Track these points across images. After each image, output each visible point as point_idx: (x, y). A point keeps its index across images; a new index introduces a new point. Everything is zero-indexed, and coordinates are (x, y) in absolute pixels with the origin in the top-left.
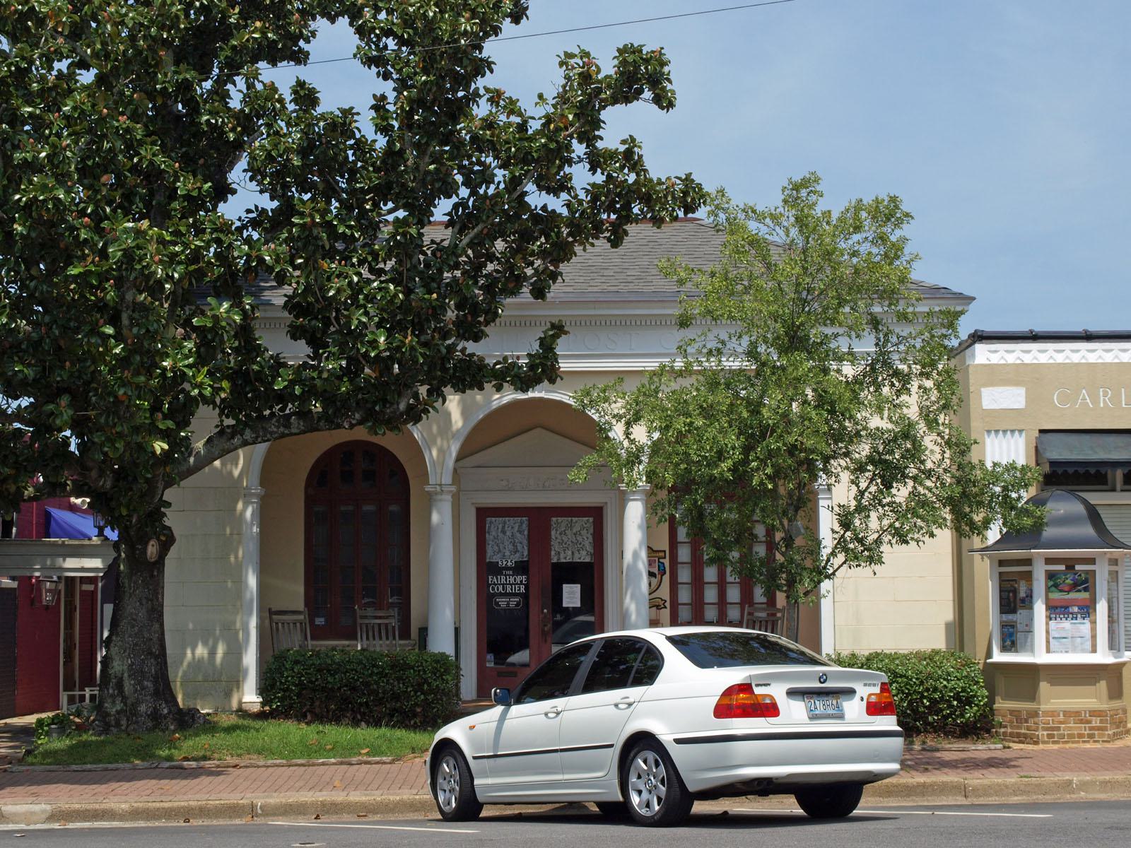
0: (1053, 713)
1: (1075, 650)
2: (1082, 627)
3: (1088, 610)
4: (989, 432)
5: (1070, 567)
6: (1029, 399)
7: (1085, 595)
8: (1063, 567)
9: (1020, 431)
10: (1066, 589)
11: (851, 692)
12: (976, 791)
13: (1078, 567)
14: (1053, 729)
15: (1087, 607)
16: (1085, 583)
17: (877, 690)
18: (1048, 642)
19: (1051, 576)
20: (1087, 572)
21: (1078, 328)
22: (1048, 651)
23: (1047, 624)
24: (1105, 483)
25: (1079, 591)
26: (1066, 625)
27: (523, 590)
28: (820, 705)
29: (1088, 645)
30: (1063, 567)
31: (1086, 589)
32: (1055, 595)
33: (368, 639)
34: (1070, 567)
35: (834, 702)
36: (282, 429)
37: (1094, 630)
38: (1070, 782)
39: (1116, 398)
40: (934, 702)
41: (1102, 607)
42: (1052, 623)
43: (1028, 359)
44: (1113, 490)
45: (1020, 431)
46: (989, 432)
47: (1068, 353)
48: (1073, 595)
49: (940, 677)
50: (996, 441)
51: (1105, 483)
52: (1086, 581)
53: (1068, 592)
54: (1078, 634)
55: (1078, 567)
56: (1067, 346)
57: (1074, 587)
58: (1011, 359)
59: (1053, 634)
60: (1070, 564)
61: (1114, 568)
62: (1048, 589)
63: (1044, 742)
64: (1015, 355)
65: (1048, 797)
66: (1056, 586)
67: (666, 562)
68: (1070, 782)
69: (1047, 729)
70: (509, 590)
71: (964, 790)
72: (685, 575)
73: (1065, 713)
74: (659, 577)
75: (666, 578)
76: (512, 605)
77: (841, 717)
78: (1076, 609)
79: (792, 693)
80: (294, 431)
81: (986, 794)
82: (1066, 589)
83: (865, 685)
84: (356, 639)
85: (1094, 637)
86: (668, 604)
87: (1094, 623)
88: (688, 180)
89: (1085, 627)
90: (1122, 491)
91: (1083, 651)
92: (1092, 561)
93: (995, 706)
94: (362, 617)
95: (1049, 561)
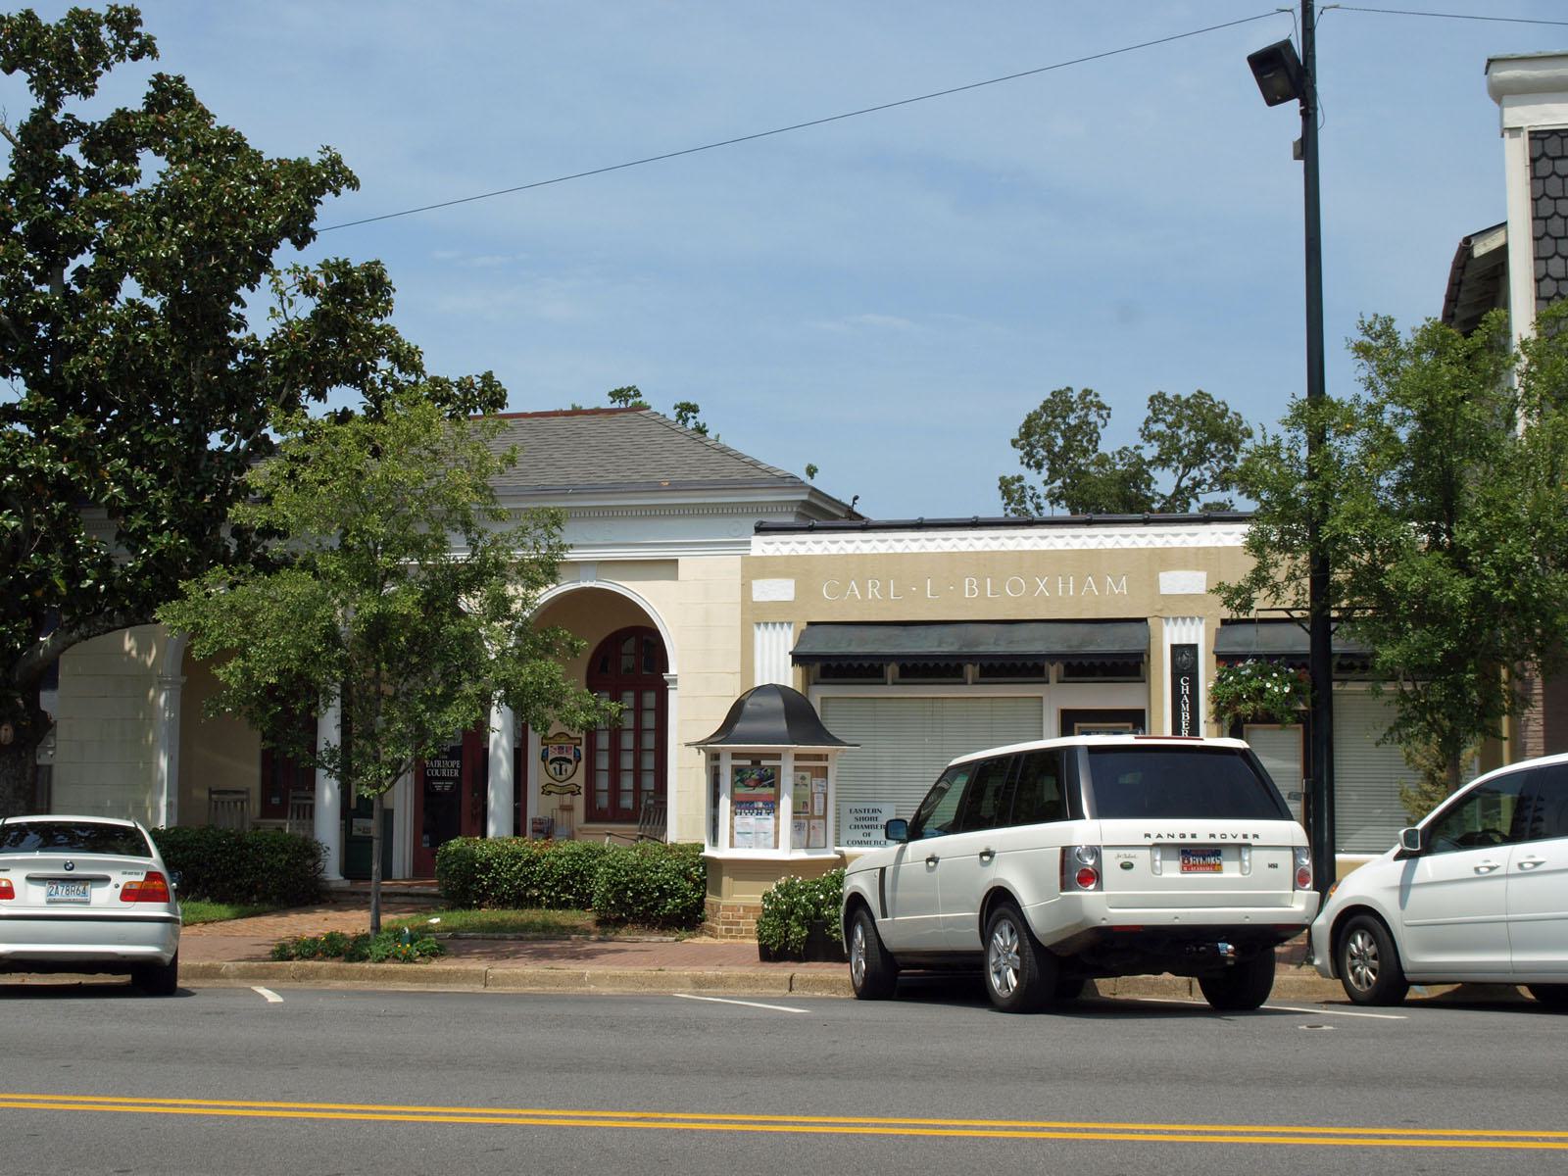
0: (733, 908)
1: (758, 845)
2: (766, 822)
3: (772, 806)
4: (759, 624)
5: (756, 763)
6: (1155, 583)
7: (771, 791)
8: (749, 763)
9: (789, 623)
10: (752, 784)
11: (107, 880)
12: (496, 981)
13: (763, 763)
14: (732, 923)
15: (772, 802)
16: (770, 779)
17: (141, 878)
18: (732, 837)
19: (737, 771)
20: (773, 767)
21: (912, 516)
22: (732, 845)
23: (732, 819)
24: (961, 676)
25: (765, 786)
26: (751, 820)
27: (456, 774)
28: (62, 891)
29: (772, 840)
30: (749, 763)
31: (772, 785)
32: (741, 791)
33: (298, 816)
34: (756, 763)
35: (81, 888)
36: (107, 624)
37: (777, 826)
38: (583, 975)
39: (884, 591)
40: (637, 894)
41: (786, 804)
42: (737, 818)
43: (802, 550)
44: (966, 683)
45: (789, 623)
46: (759, 624)
47: (826, 544)
48: (759, 790)
49: (646, 869)
50: (767, 634)
51: (961, 676)
52: (772, 776)
53: (754, 787)
54: (762, 830)
55: (763, 763)
56: (939, 534)
57: (760, 782)
58: (785, 551)
59: (738, 829)
60: (756, 759)
61: (715, 763)
62: (734, 785)
63: (722, 937)
64: (1130, 539)
65: (560, 988)
66: (742, 781)
67: (582, 749)
68: (583, 975)
69: (724, 923)
70: (444, 774)
71: (484, 978)
72: (603, 762)
73: (745, 908)
74: (574, 763)
75: (582, 765)
76: (447, 788)
77: (87, 902)
78: (761, 805)
79: (29, 879)
80: (117, 625)
81: (504, 984)
82: (752, 784)
83: (125, 873)
84: (285, 817)
85: (777, 833)
86: (582, 791)
87: (777, 818)
88: (488, 378)
89: (768, 822)
90: (894, 684)
91: (766, 847)
92: (777, 756)
93: (706, 899)
94: (294, 798)
95: (735, 756)
